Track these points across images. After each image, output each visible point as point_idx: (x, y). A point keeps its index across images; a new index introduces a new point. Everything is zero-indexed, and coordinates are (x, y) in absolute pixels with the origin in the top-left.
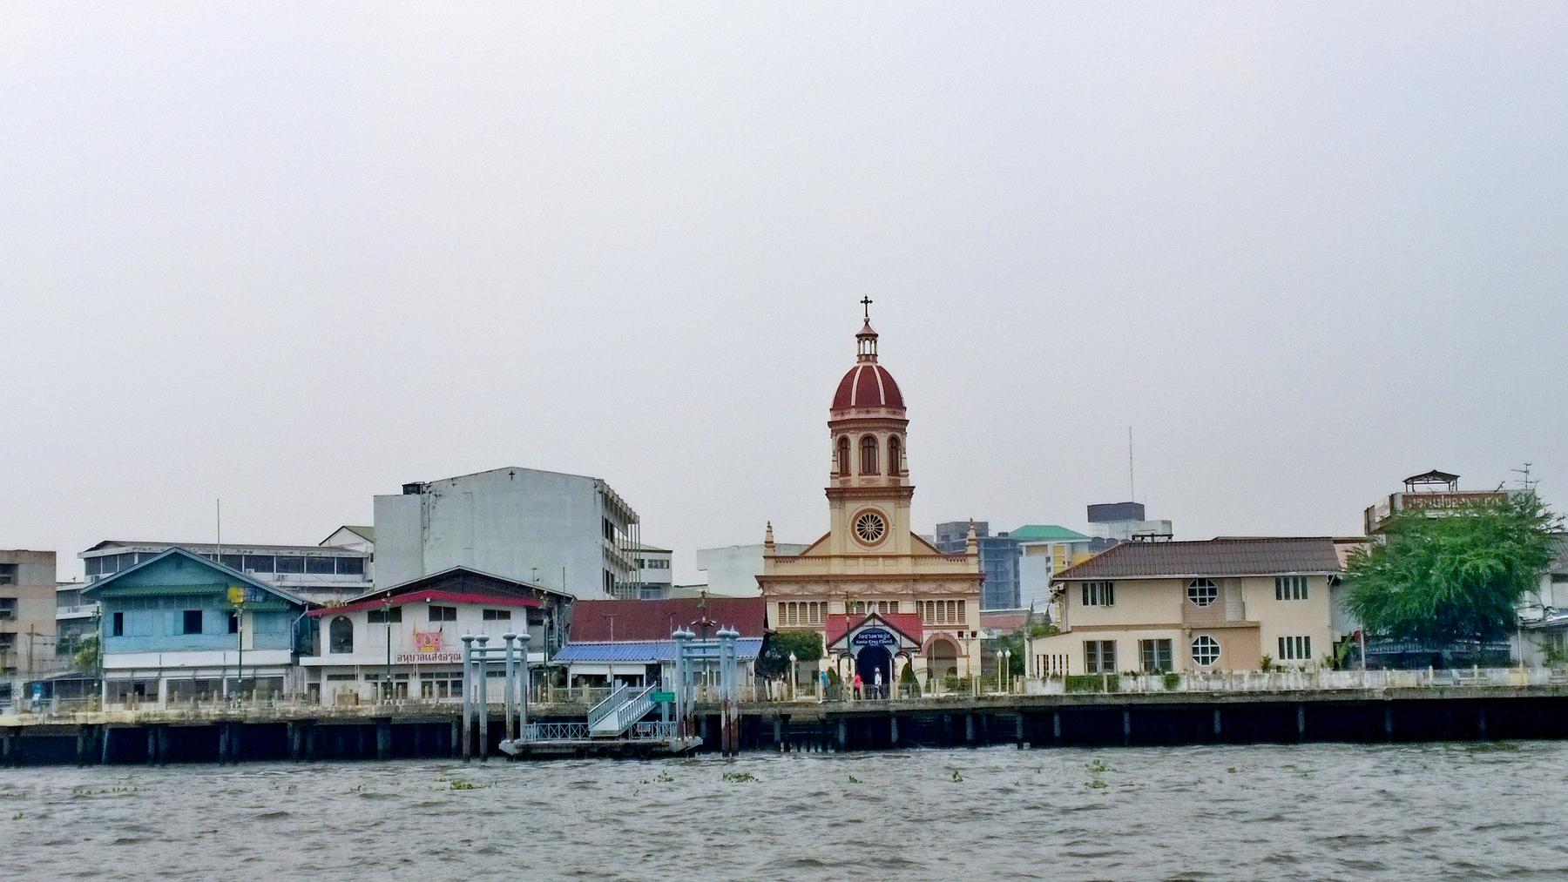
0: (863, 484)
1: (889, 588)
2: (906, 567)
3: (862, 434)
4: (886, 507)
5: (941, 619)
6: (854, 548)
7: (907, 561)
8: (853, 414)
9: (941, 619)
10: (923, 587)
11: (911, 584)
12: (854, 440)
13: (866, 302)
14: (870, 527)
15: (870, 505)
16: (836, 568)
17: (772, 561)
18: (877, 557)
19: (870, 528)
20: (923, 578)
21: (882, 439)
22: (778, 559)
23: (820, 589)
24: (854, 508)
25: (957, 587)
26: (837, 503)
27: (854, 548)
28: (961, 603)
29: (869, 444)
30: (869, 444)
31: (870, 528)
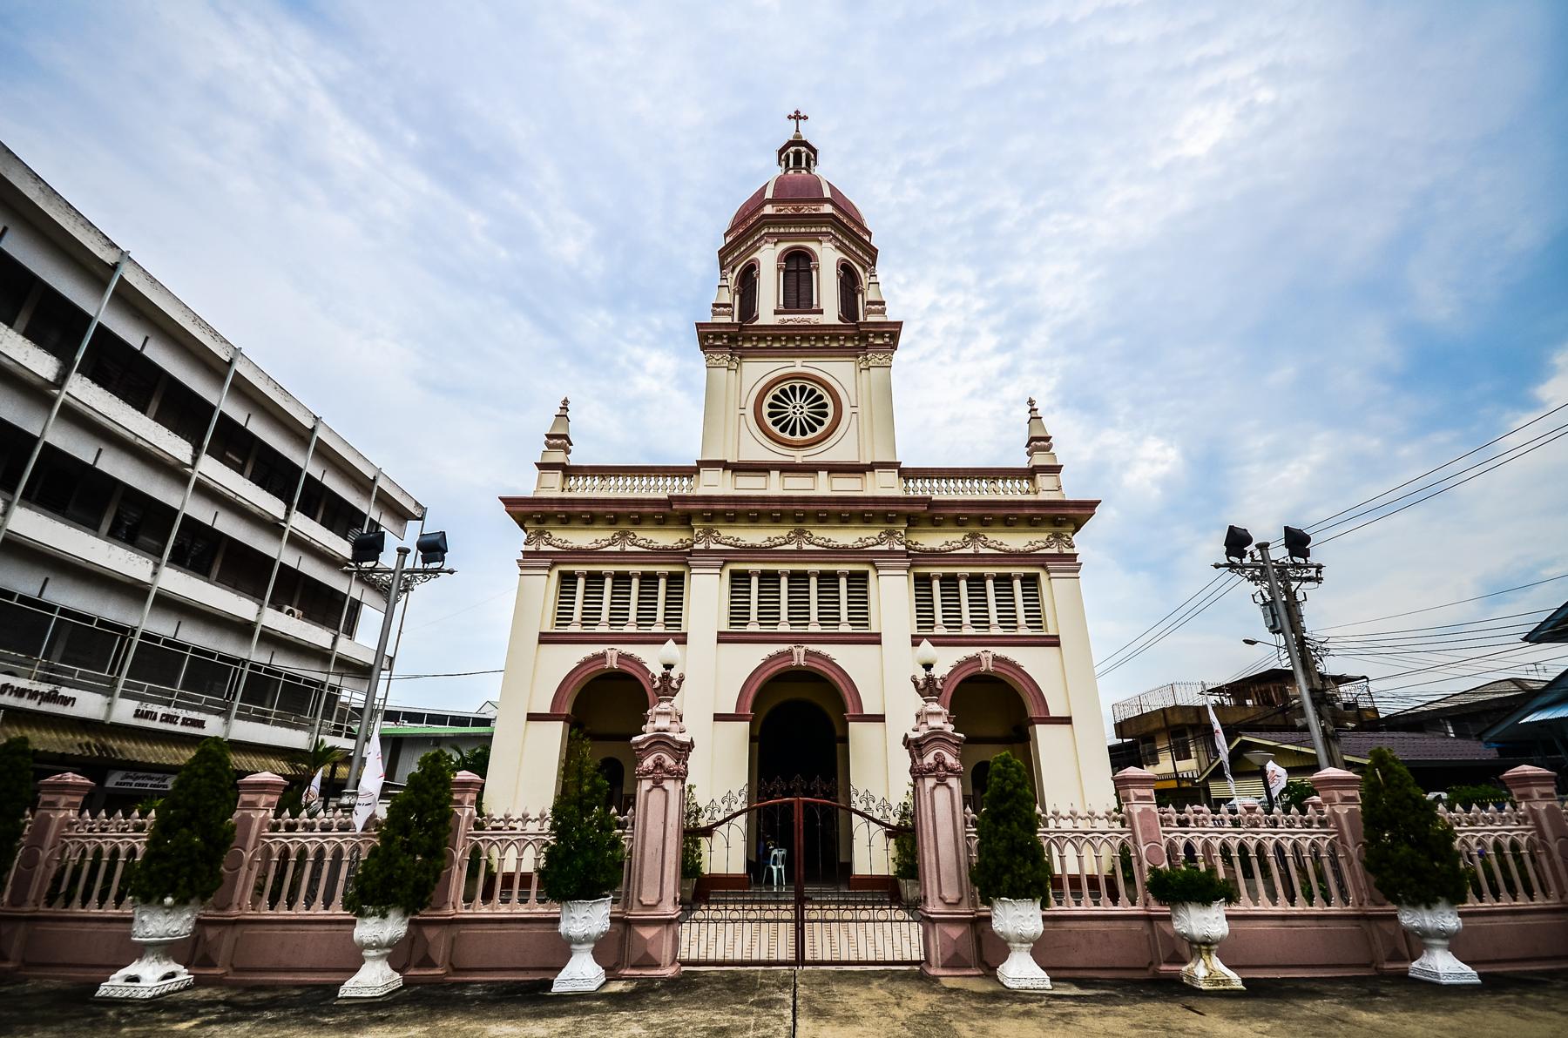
1: (846, 537)
3: (783, 246)
5: (981, 620)
6: (758, 449)
8: (769, 210)
9: (981, 620)
10: (932, 540)
12: (768, 258)
13: (797, 117)
14: (798, 409)
15: (798, 365)
17: (556, 478)
18: (811, 469)
19: (798, 413)
21: (828, 257)
22: (568, 471)
23: (667, 539)
24: (759, 371)
25: (1017, 541)
26: (722, 359)
28: (1031, 582)
29: (798, 267)
30: (798, 267)
31: (798, 413)
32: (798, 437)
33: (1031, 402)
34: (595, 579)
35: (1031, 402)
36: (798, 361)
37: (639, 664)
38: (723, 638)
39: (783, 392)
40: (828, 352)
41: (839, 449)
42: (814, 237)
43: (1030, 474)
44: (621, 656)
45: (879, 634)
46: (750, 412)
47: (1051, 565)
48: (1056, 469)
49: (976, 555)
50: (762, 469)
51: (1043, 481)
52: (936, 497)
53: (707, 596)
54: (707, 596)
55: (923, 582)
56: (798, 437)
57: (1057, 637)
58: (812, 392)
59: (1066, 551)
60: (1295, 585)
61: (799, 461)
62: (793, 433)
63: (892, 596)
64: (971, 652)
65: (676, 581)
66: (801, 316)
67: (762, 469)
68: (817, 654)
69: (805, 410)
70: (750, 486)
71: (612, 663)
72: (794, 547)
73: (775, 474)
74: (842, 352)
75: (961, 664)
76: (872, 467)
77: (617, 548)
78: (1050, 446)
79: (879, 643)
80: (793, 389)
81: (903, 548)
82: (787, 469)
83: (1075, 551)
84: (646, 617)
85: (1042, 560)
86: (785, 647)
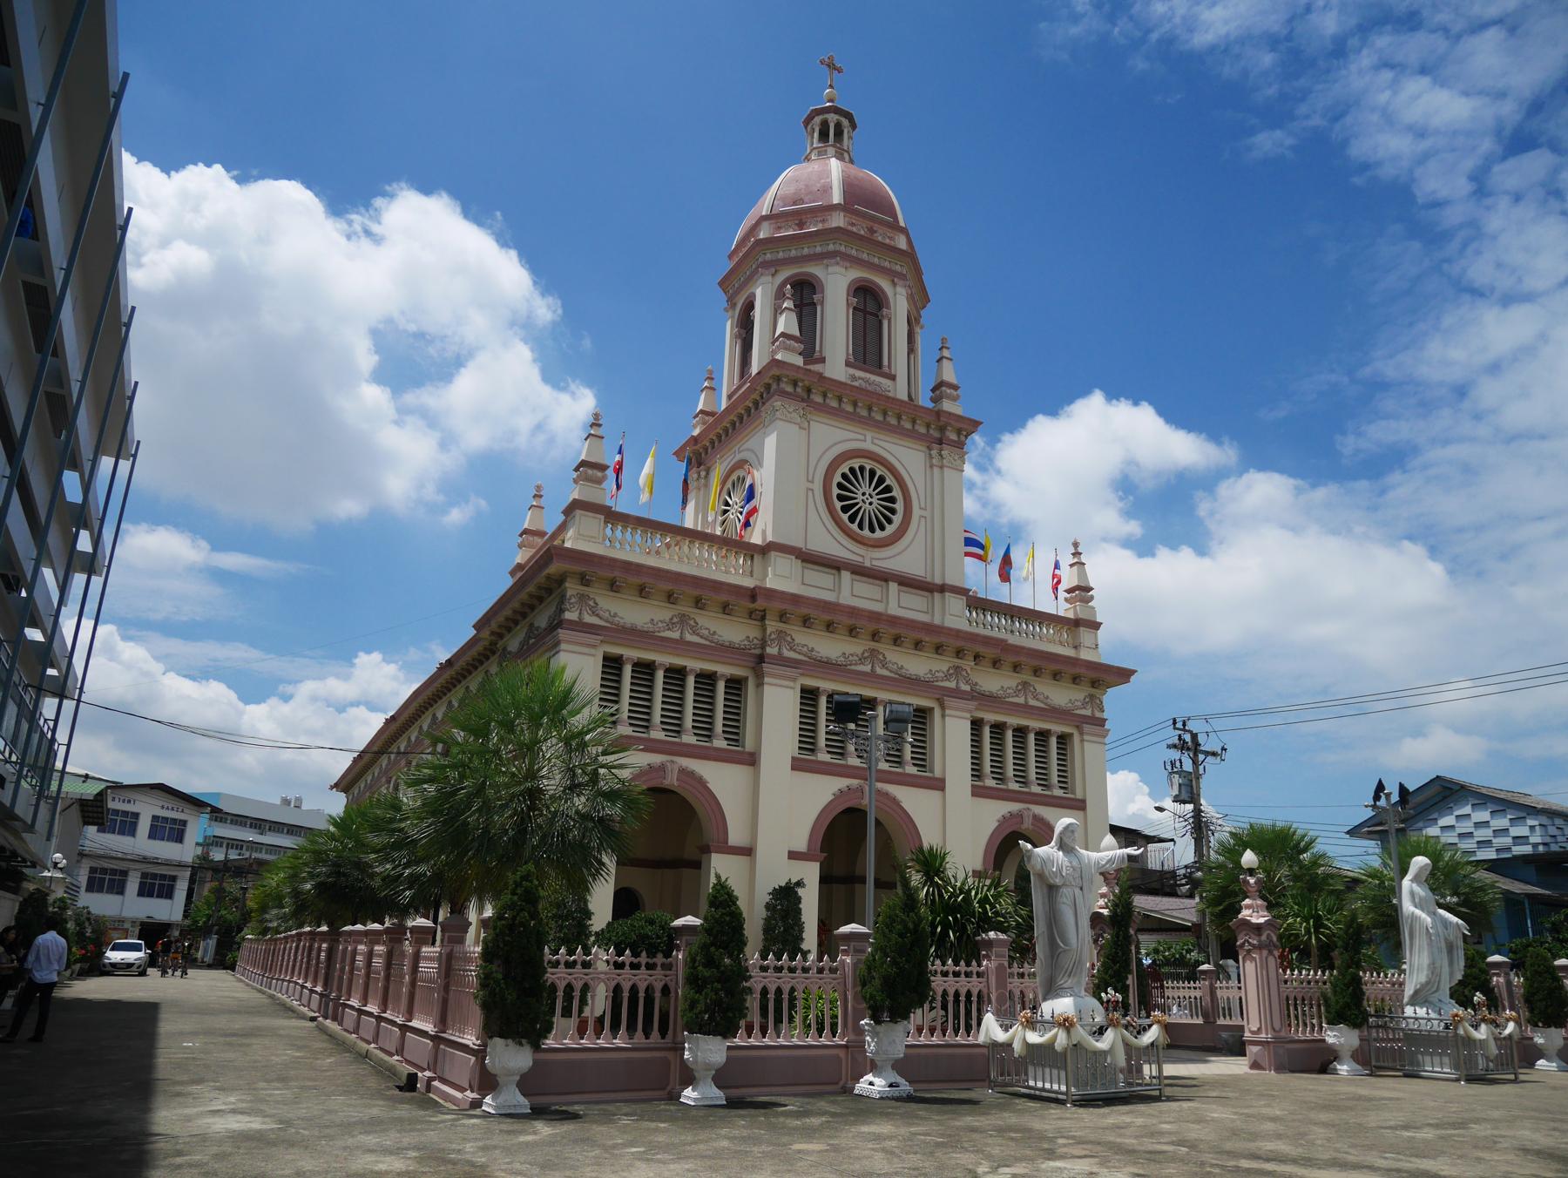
0: (856, 384)
1: (918, 665)
2: (955, 616)
4: (907, 458)
6: (827, 540)
7: (956, 604)
11: (967, 664)
12: (836, 284)
15: (869, 440)
16: (781, 577)
18: (883, 577)
20: (999, 655)
23: (735, 632)
27: (827, 540)
28: (1063, 740)
30: (868, 303)
31: (864, 499)
32: (866, 532)
33: (1076, 545)
34: (645, 670)
35: (1076, 545)
36: (869, 435)
37: (702, 782)
38: (797, 765)
39: (852, 470)
40: (897, 431)
41: (906, 558)
42: (893, 276)
43: (1076, 623)
44: (684, 772)
45: (943, 781)
46: (818, 486)
47: (1087, 728)
48: (1096, 626)
49: (1026, 706)
50: (833, 565)
51: (1085, 635)
52: (1013, 640)
53: (777, 711)
54: (777, 711)
55: (976, 725)
56: (855, 527)
57: (1084, 801)
58: (882, 480)
59: (1098, 714)
60: (1201, 757)
61: (867, 564)
62: (861, 526)
63: (953, 738)
64: (1014, 807)
65: (736, 686)
66: (868, 375)
67: (833, 565)
68: (887, 794)
69: (874, 500)
70: (818, 586)
71: (671, 781)
72: (867, 668)
73: (846, 576)
74: (912, 435)
75: (1005, 820)
76: (942, 589)
77: (675, 635)
78: (1092, 598)
79: (943, 789)
80: (862, 469)
81: (967, 688)
82: (859, 571)
83: (1105, 715)
84: (705, 728)
85: (1081, 722)
86: (855, 782)
